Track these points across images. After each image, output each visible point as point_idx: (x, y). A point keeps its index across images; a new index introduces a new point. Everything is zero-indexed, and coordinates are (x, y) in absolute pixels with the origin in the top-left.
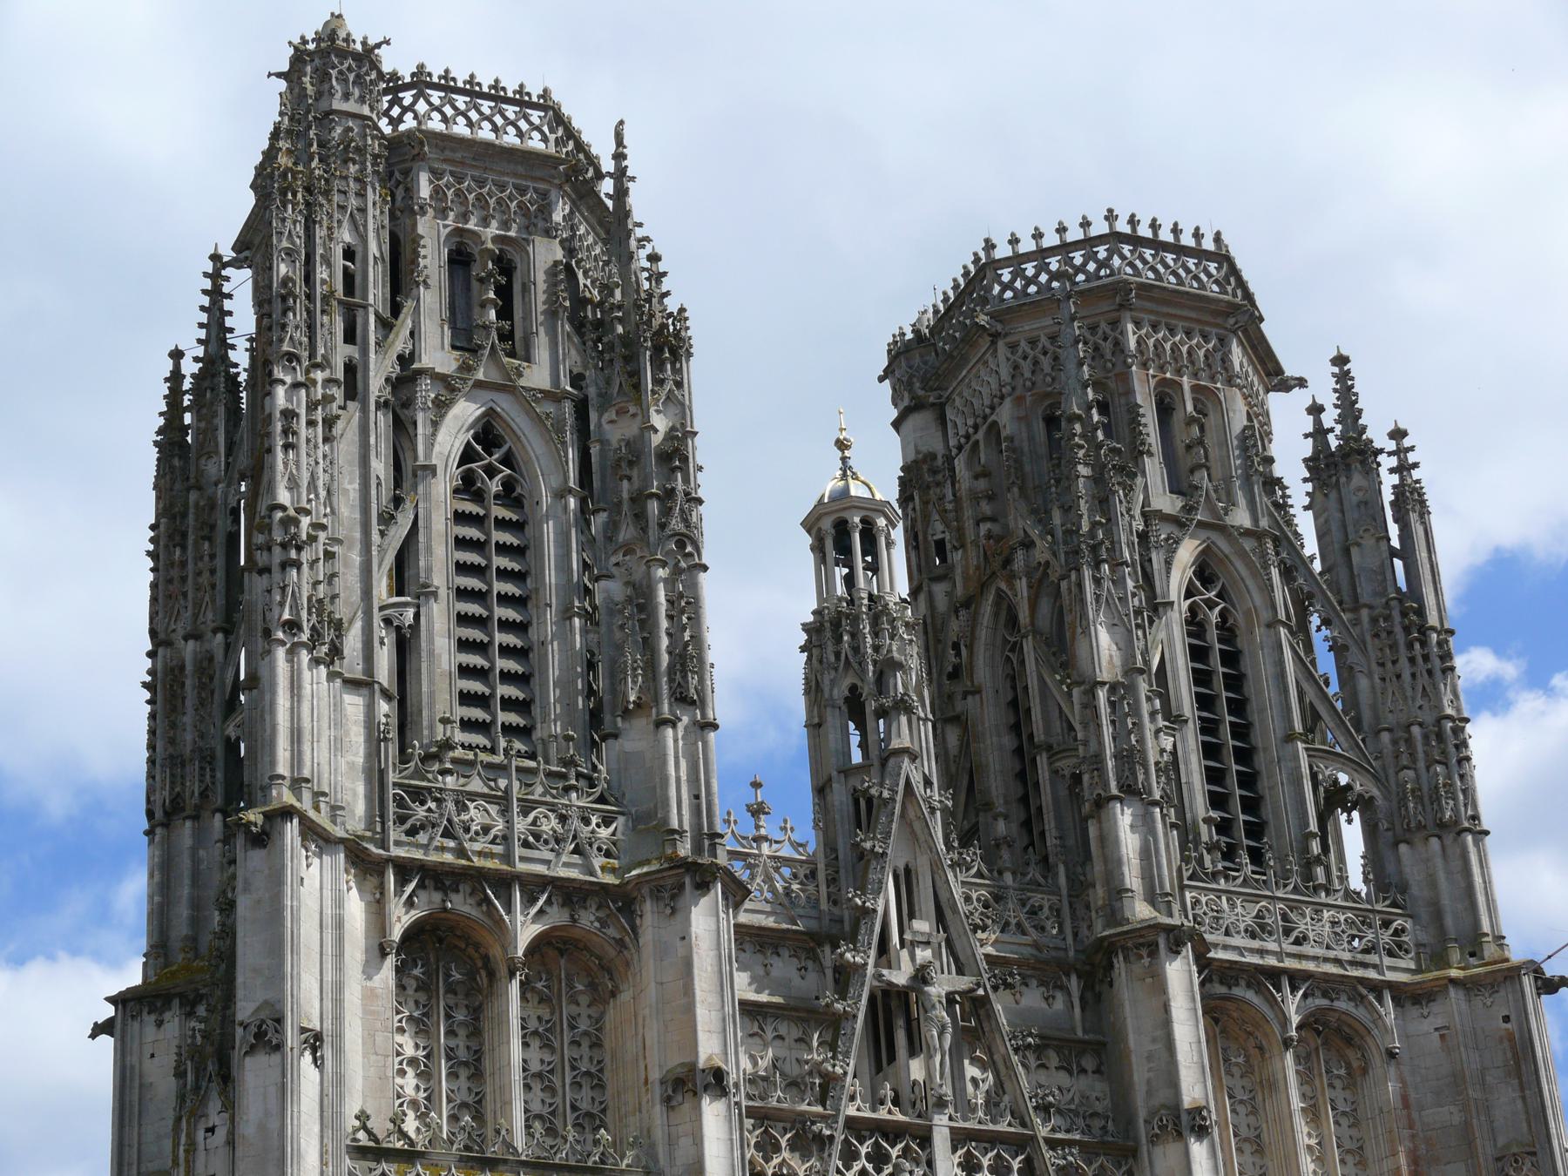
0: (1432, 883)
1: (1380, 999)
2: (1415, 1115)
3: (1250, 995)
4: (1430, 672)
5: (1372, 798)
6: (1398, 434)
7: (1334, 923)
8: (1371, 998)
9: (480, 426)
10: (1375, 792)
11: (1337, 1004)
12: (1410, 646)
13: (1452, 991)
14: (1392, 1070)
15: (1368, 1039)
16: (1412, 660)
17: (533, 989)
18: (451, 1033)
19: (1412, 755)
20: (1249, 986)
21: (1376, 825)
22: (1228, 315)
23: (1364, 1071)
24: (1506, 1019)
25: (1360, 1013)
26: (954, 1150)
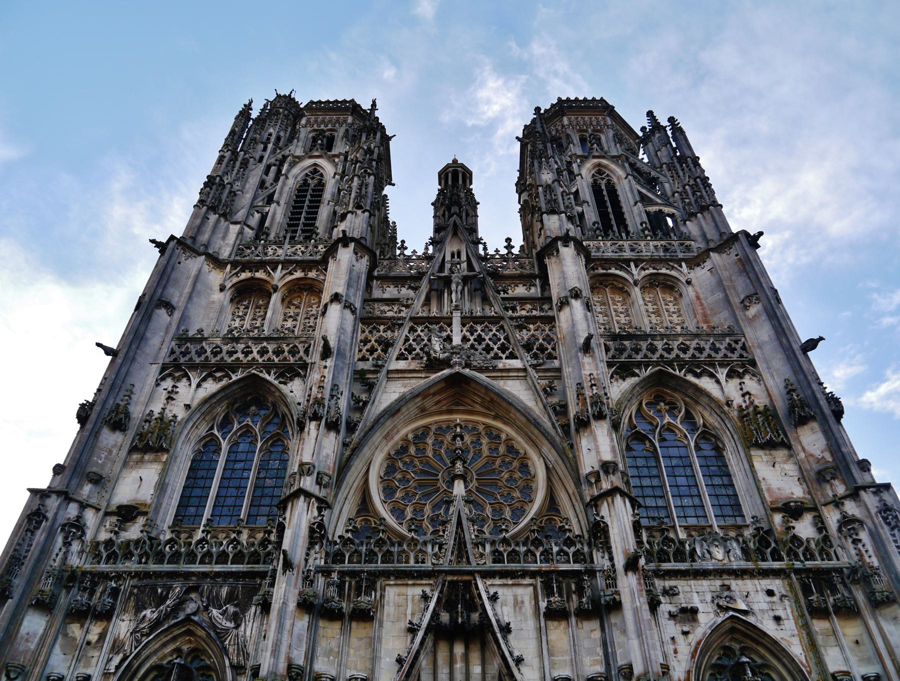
0: (701, 228)
1: (681, 266)
2: (703, 302)
3: (618, 272)
4: (690, 170)
5: (674, 214)
6: (671, 120)
7: (656, 247)
8: (675, 265)
9: (311, 169)
10: (674, 211)
11: (660, 271)
12: (681, 166)
13: (711, 254)
14: (690, 289)
15: (679, 283)
16: (683, 170)
17: (294, 305)
18: (254, 319)
19: (687, 195)
20: (616, 269)
21: (677, 221)
22: (605, 112)
23: (681, 295)
24: (737, 255)
25: (673, 273)
26: (464, 325)
